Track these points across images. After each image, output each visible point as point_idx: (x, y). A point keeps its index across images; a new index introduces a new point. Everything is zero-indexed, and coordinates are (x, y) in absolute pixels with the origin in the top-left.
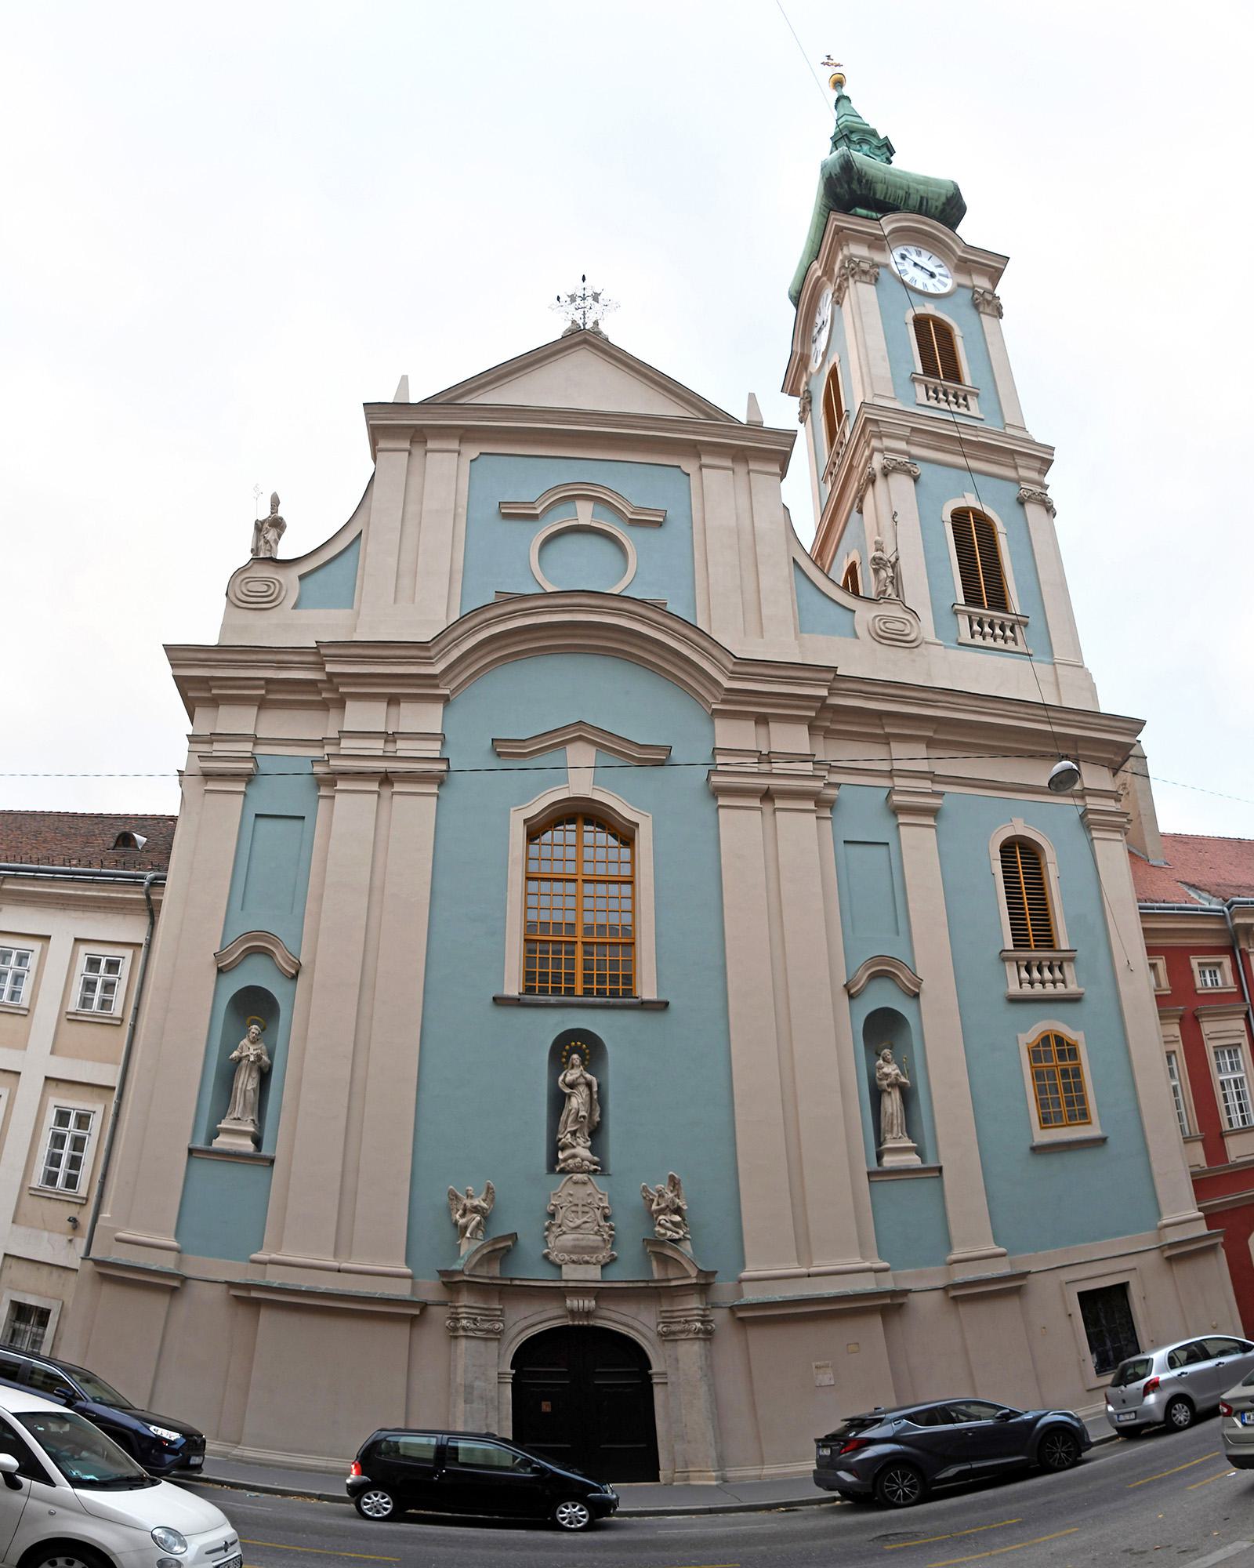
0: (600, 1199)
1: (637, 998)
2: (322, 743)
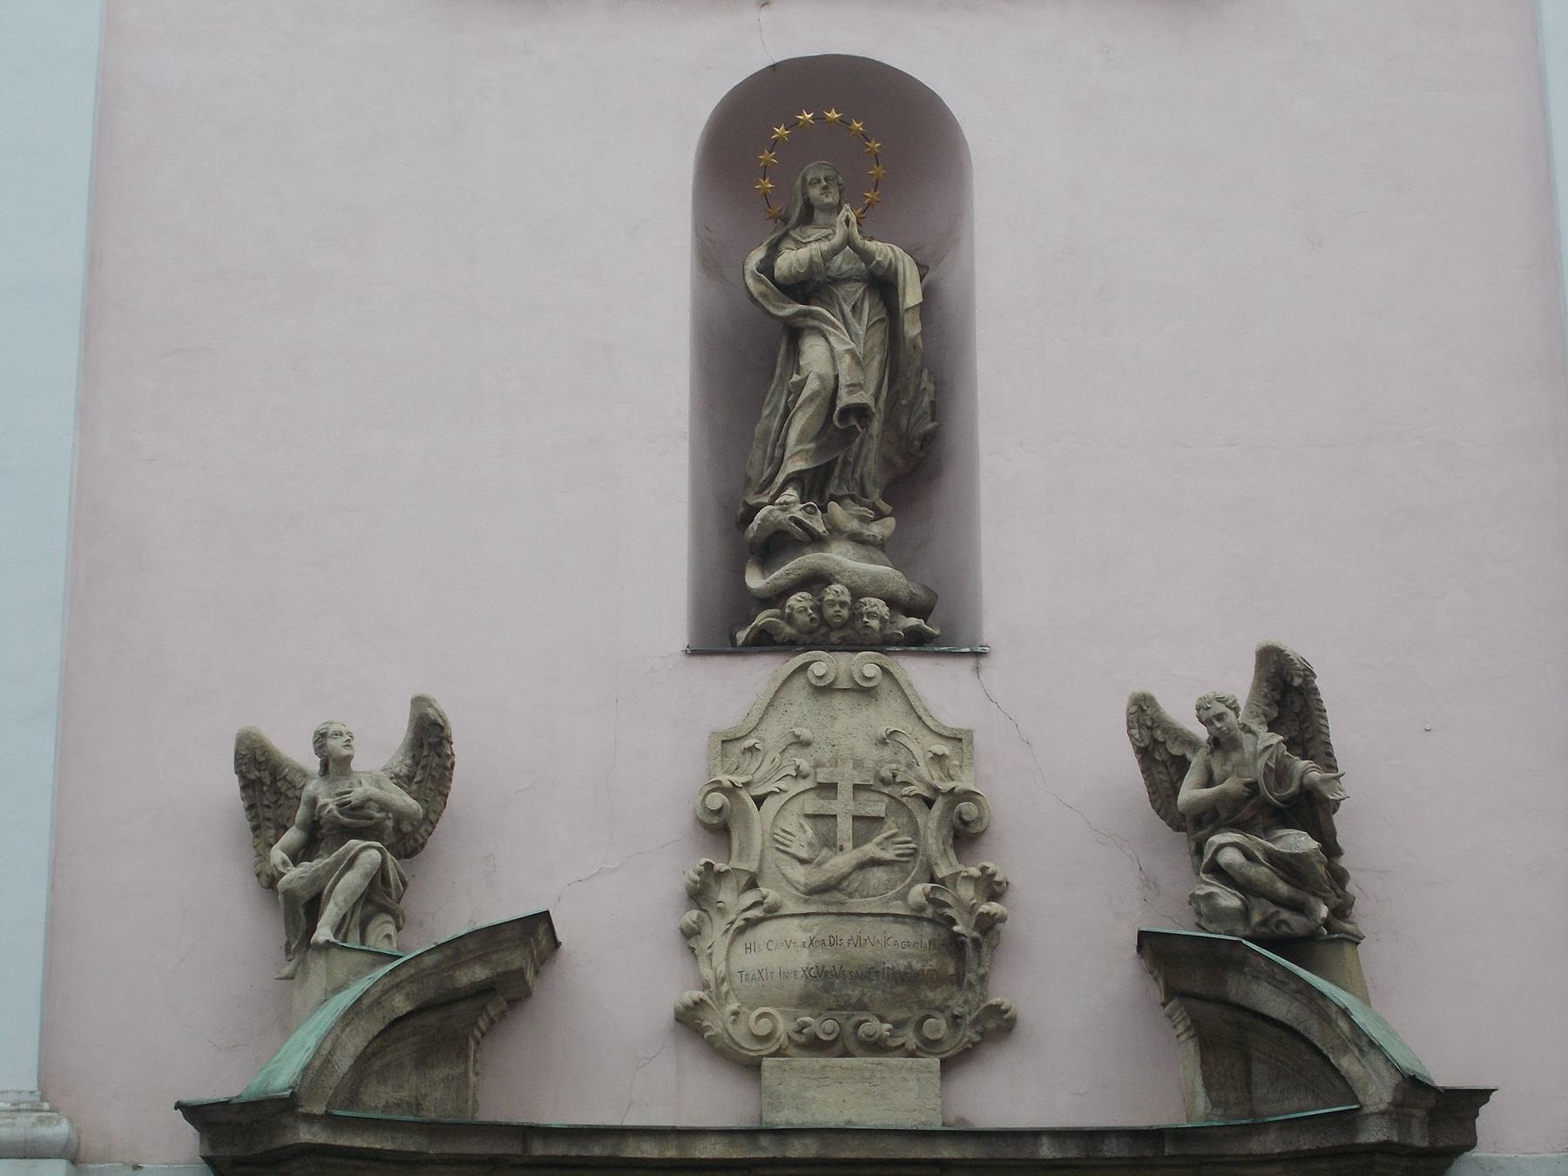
0: (938, 758)
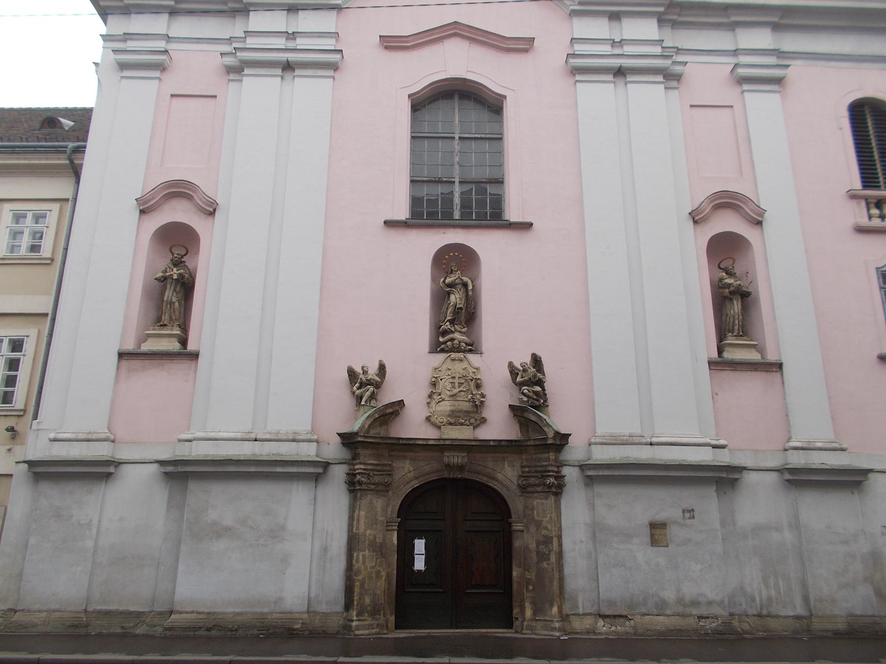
0: (474, 372)
1: (507, 220)
2: (230, 40)
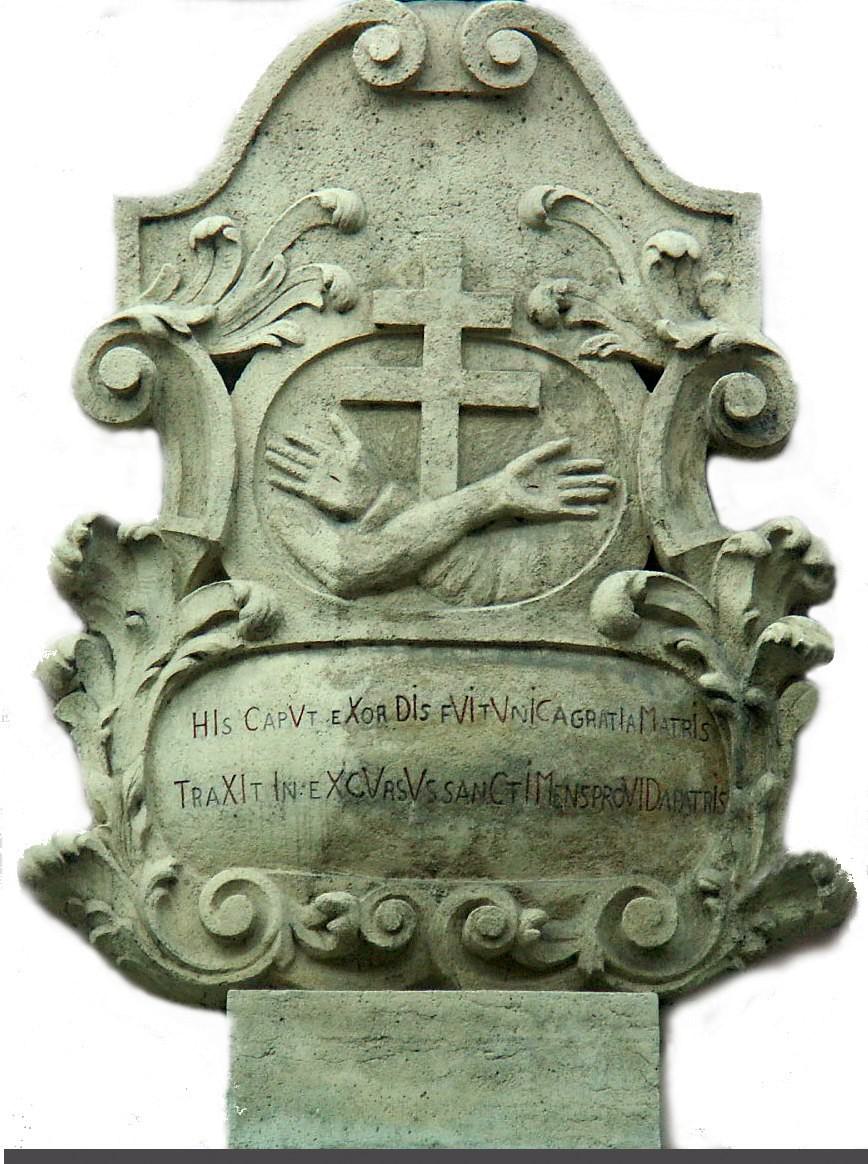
0: (673, 264)
